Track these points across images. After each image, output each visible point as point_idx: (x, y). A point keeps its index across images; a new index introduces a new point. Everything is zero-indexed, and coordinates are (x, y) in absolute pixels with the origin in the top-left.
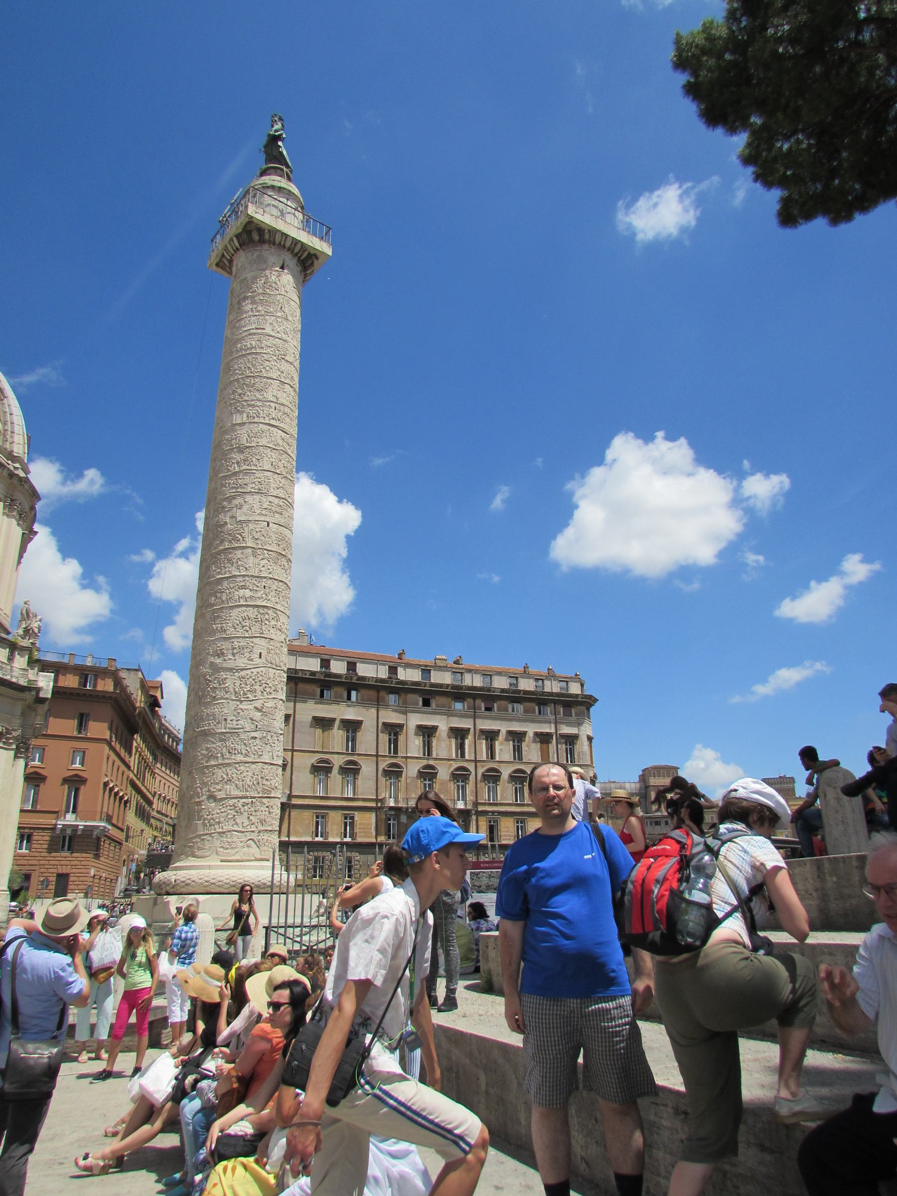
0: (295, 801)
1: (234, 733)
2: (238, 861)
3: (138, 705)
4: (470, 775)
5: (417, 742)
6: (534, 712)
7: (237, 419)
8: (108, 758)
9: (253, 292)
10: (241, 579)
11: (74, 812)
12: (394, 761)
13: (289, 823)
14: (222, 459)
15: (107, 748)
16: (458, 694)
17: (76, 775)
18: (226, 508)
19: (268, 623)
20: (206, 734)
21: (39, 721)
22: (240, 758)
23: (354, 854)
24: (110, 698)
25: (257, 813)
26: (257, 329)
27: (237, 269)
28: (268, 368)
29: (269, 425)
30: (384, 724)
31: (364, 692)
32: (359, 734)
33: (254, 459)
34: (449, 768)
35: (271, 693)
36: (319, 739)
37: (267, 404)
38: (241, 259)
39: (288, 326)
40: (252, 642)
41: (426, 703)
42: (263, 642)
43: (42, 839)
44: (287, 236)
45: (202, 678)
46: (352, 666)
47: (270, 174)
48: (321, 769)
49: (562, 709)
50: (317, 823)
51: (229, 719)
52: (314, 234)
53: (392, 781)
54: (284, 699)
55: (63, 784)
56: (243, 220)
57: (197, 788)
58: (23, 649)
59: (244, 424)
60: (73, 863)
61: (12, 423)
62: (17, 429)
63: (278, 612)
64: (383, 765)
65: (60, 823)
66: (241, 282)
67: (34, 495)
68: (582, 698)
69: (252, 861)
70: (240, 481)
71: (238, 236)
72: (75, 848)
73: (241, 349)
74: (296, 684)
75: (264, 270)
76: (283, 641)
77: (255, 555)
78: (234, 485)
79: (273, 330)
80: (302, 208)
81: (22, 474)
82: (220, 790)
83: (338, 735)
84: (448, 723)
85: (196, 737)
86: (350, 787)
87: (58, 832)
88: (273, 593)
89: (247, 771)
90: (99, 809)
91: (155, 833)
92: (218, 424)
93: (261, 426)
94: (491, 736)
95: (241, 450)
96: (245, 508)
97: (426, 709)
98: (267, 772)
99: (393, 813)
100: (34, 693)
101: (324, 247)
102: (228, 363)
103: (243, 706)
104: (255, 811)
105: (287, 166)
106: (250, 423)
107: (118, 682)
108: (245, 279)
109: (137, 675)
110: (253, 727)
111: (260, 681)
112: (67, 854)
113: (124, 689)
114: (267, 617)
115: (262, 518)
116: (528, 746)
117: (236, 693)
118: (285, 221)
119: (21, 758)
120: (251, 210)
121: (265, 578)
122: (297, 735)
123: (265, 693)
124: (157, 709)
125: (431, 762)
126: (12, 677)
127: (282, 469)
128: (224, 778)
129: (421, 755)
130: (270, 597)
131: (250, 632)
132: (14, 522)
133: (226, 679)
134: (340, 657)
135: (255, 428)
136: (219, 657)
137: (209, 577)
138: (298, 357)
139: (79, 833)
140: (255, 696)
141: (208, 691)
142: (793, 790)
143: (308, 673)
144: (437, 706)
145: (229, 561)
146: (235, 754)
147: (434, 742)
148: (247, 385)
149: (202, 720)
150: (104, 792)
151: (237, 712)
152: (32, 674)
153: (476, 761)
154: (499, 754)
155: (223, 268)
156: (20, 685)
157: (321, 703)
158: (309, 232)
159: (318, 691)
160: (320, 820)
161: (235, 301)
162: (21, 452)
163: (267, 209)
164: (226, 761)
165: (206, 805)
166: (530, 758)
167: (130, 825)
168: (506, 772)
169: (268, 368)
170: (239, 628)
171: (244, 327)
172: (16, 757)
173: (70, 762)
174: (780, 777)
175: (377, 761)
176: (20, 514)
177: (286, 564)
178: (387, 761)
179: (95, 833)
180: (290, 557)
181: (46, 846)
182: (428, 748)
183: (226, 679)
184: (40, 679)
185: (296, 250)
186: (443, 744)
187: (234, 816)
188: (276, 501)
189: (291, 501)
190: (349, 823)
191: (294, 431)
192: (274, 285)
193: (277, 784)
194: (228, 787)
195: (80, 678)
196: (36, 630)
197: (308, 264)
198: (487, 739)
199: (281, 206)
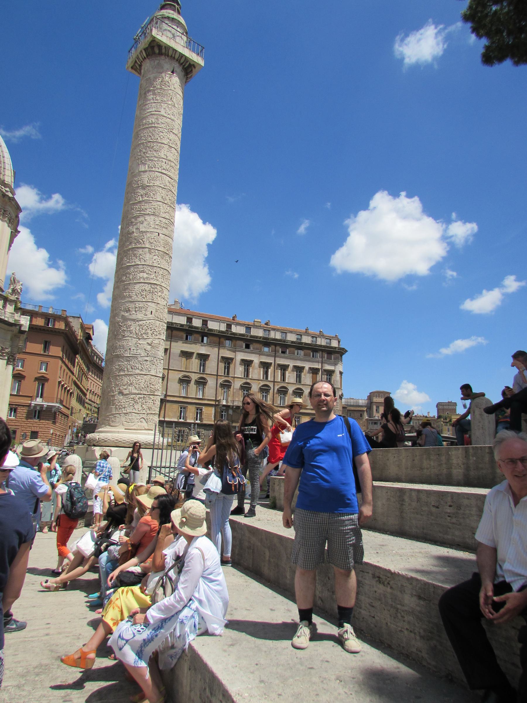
0: (168, 398)
1: (135, 357)
2: (135, 430)
3: (79, 338)
4: (270, 389)
5: (241, 369)
6: (310, 356)
7: (142, 168)
8: (61, 368)
9: (154, 87)
10: (141, 266)
11: (41, 397)
12: (227, 379)
13: (165, 410)
14: (132, 193)
15: (60, 362)
16: (266, 342)
17: (43, 376)
18: (133, 223)
19: (157, 294)
20: (118, 356)
21: (21, 344)
22: (137, 371)
23: (201, 430)
24: (63, 333)
25: (147, 404)
26: (156, 111)
27: (144, 71)
28: (161, 137)
29: (161, 173)
30: (222, 357)
31: (211, 338)
32: (207, 362)
33: (151, 194)
34: (259, 385)
35: (157, 335)
36: (184, 364)
37: (161, 160)
38: (147, 65)
39: (175, 111)
40: (147, 305)
41: (247, 347)
42: (153, 305)
43: (22, 412)
44: (176, 51)
45: (116, 323)
46: (205, 323)
47: (167, 9)
48: (185, 381)
49: (326, 355)
50: (181, 411)
51: (132, 349)
52: (193, 51)
53: (225, 390)
54: (165, 339)
55: (35, 381)
56: (149, 39)
57: (112, 387)
58: (11, 301)
59: (146, 171)
60: (40, 426)
61: (4, 163)
62: (7, 167)
63: (163, 288)
64: (220, 381)
65: (33, 403)
66: (147, 80)
67: (18, 208)
68: (338, 349)
69: (143, 430)
70: (142, 207)
71: (146, 50)
72: (42, 417)
73: (146, 124)
74: (172, 331)
75: (161, 73)
76: (165, 305)
77: (150, 253)
78: (139, 209)
79: (165, 113)
80: (187, 33)
81: (10, 195)
82: (126, 389)
83: (195, 363)
84: (259, 360)
85: (112, 358)
86: (201, 393)
87: (32, 408)
88: (160, 276)
89: (142, 379)
90: (56, 396)
91: (88, 412)
92: (130, 170)
93: (157, 173)
94: (284, 368)
95: (144, 187)
96: (145, 223)
97: (247, 350)
98: (153, 380)
99: (225, 408)
100: (18, 327)
101: (199, 60)
102: (137, 132)
103: (141, 342)
104: (146, 402)
105: (178, 4)
106: (150, 171)
107: (67, 324)
108: (149, 78)
109: (79, 320)
110: (146, 354)
111: (151, 328)
112: (37, 420)
113: (71, 328)
114: (156, 290)
115: (156, 230)
116: (305, 375)
117: (136, 334)
118: (175, 42)
119: (11, 364)
120: (154, 32)
121: (156, 267)
122: (171, 361)
123: (153, 335)
124: (90, 341)
125: (248, 381)
126: (5, 317)
127: (168, 201)
128: (128, 383)
129: (243, 377)
130: (158, 278)
131: (146, 299)
132: (6, 225)
133: (131, 325)
134: (198, 317)
135: (153, 175)
136: (127, 312)
137: (122, 265)
138: (180, 131)
139: (44, 409)
140: (148, 336)
141: (120, 332)
142: (455, 410)
143: (179, 325)
144: (254, 349)
145: (135, 255)
146: (135, 369)
147: (251, 370)
148: (149, 147)
149: (116, 348)
150: (59, 387)
151: (137, 345)
152: (17, 316)
153: (274, 382)
154: (288, 378)
155: (136, 70)
156: (10, 323)
157: (186, 343)
158: (190, 49)
159: (185, 336)
160: (182, 410)
161: (143, 92)
162: (10, 181)
163: (165, 33)
164: (130, 373)
165: (117, 397)
166: (306, 382)
167: (73, 406)
168: (291, 389)
169: (161, 137)
170: (139, 296)
171: (148, 109)
172: (7, 364)
173: (39, 369)
174: (449, 402)
175: (217, 378)
176: (10, 220)
177: (168, 259)
178: (222, 378)
179: (53, 410)
180: (171, 255)
181: (25, 416)
182: (247, 373)
183: (131, 325)
184: (22, 319)
185: (182, 61)
186: (256, 371)
187: (133, 404)
188: (164, 220)
189: (173, 221)
190: (199, 413)
191: (176, 178)
192: (167, 83)
193: (158, 388)
194: (130, 388)
195: (45, 320)
196: (19, 291)
197: (188, 71)
198: (281, 370)
199: (173, 31)
